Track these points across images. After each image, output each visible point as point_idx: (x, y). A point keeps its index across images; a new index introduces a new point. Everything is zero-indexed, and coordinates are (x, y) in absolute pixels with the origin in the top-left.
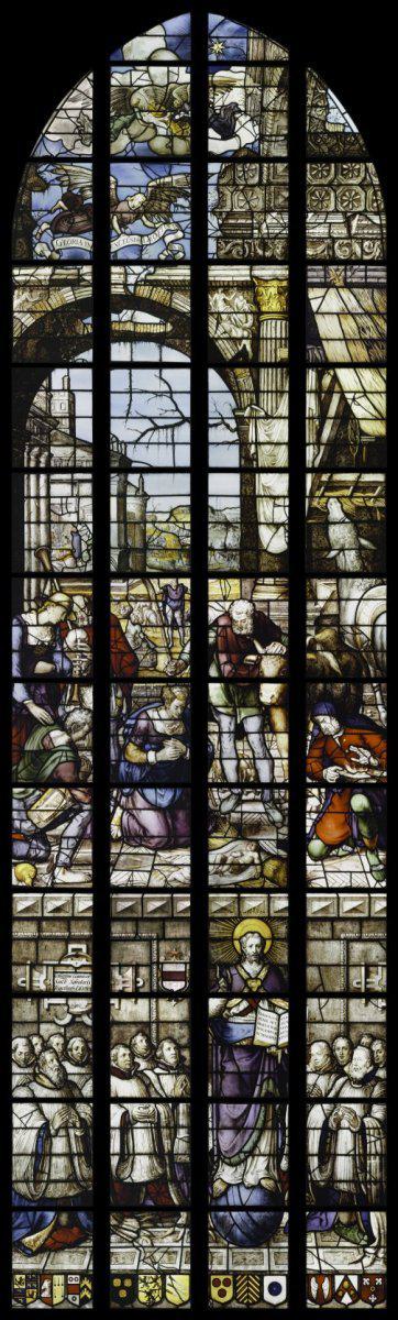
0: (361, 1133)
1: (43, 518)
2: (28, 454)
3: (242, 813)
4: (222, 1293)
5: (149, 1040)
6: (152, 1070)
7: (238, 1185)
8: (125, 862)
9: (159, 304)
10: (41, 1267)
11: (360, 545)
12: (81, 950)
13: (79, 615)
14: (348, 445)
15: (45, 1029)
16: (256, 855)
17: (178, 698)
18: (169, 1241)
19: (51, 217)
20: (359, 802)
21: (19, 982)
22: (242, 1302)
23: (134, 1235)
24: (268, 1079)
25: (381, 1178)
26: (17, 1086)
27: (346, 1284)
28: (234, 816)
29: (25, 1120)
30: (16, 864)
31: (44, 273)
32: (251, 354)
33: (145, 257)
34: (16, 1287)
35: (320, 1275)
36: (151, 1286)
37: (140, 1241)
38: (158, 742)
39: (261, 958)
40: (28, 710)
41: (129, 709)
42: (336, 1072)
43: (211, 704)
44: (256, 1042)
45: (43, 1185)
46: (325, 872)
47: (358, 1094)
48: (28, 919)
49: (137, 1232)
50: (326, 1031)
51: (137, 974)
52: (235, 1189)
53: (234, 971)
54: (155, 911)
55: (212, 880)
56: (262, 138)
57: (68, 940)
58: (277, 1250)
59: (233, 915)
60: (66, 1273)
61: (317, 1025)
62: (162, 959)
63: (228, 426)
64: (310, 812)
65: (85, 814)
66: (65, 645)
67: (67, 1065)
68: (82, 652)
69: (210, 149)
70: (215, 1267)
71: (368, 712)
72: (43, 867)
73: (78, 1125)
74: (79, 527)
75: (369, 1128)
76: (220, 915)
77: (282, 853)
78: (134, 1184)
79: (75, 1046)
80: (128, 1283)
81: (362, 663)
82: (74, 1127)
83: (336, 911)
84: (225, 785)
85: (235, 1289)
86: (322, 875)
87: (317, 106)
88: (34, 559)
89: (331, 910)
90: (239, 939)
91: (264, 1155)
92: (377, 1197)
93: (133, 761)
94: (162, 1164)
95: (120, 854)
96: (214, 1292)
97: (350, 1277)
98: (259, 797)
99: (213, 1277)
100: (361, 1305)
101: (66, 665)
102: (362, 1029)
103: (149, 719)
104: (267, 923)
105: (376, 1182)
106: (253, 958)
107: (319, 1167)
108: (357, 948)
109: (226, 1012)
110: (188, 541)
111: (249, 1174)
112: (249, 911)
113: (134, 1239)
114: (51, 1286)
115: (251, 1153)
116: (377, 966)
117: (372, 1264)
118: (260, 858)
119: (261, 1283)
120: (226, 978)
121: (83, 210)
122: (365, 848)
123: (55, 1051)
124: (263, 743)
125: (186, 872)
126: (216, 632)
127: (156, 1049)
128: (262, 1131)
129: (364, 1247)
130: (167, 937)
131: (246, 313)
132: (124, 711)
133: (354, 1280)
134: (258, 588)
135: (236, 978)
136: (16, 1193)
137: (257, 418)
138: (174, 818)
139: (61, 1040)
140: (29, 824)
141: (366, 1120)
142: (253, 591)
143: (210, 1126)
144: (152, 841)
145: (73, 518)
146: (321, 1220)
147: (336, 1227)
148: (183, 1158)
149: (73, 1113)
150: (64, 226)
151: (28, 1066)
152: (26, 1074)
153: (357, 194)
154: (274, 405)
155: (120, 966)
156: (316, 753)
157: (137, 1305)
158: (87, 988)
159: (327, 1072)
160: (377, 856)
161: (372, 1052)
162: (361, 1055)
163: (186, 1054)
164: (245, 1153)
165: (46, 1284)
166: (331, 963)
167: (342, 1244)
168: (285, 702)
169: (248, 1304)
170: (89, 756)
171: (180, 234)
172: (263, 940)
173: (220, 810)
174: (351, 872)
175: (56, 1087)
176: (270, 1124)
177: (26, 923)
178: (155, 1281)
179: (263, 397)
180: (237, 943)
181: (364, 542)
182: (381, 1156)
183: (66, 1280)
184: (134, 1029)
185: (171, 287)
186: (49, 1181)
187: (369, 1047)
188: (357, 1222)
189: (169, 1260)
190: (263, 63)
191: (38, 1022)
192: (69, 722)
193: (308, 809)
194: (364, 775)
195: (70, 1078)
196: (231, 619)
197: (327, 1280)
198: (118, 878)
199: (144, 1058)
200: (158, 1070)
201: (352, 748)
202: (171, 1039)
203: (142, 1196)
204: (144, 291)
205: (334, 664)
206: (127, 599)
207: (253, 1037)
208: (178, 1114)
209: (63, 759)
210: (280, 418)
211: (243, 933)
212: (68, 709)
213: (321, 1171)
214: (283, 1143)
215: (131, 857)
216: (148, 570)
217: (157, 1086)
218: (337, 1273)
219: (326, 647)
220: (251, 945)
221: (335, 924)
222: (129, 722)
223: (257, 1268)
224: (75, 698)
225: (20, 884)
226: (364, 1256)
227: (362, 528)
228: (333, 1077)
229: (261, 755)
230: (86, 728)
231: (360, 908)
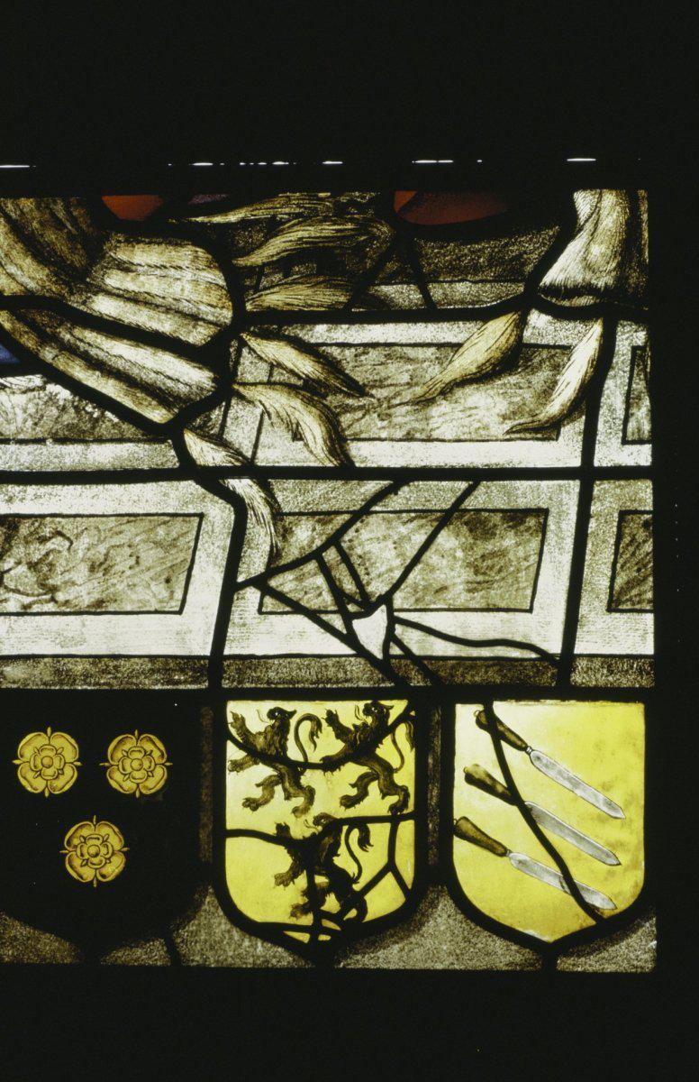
23: (193, 377)
36: (330, 791)
37: (241, 426)
178: (361, 746)
189: (484, 572)
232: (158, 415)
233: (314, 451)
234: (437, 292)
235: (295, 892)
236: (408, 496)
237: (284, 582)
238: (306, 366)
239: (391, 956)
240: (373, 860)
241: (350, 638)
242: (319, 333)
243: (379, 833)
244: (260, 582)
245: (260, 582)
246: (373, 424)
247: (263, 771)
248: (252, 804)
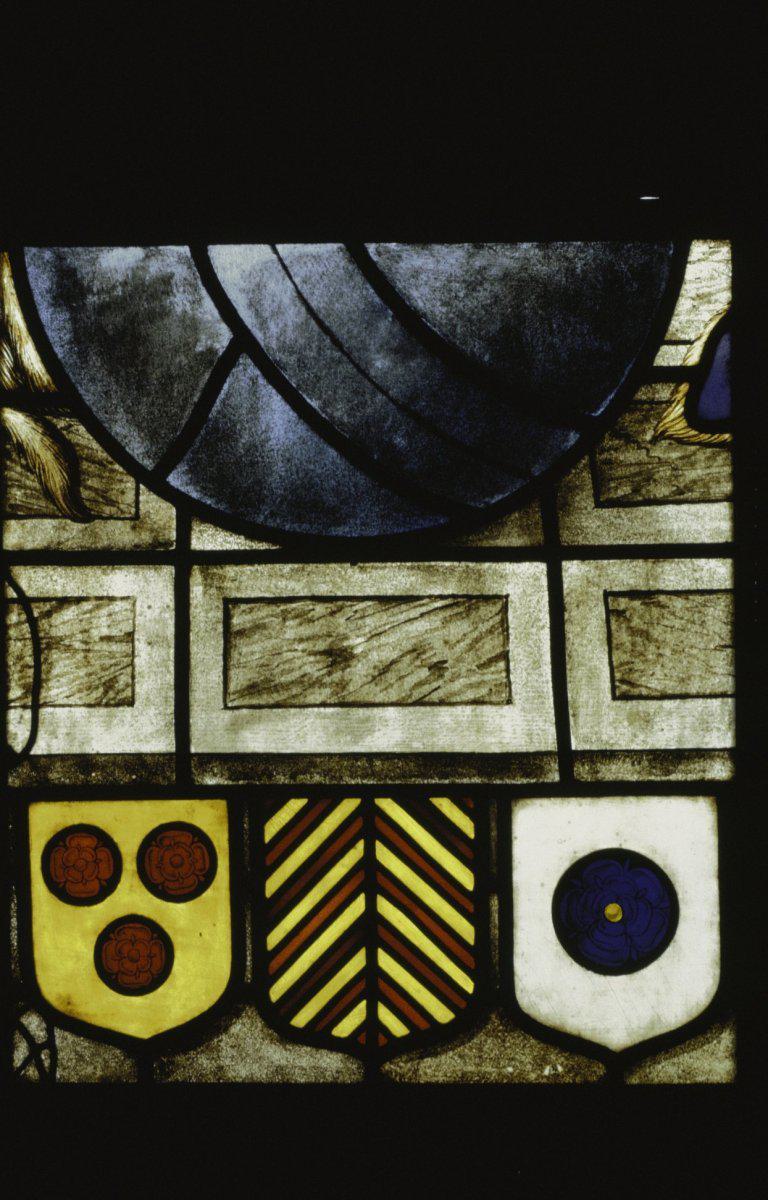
22: (318, 1036)
58: (625, 574)
99: (45, 820)
169: (370, 1044)
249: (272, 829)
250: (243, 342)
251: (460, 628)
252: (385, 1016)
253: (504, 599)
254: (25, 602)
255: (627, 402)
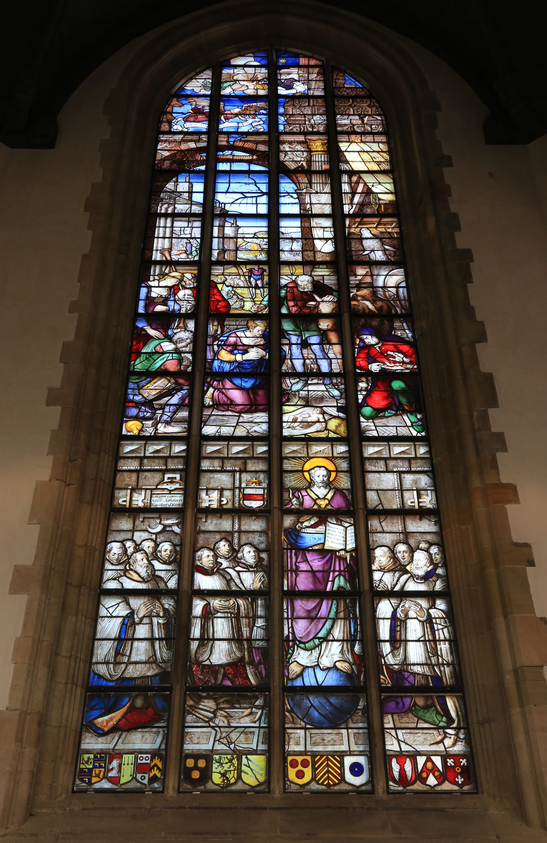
0: (429, 621)
1: (168, 235)
2: (161, 207)
3: (308, 391)
4: (300, 775)
5: (231, 545)
6: (233, 568)
7: (313, 667)
8: (214, 420)
9: (249, 148)
10: (111, 746)
11: (385, 248)
12: (175, 478)
13: (188, 283)
14: (372, 204)
15: (138, 536)
16: (321, 416)
17: (259, 328)
18: (246, 722)
19: (184, 116)
20: (397, 385)
21: (120, 501)
22: (322, 784)
23: (211, 715)
24: (339, 575)
25: (453, 661)
26: (108, 580)
27: (429, 765)
28: (303, 393)
29: (111, 610)
30: (126, 421)
31: (179, 137)
32: (306, 167)
33: (240, 130)
34: (82, 766)
35: (401, 756)
36: (226, 767)
37: (217, 721)
38: (245, 349)
39: (328, 484)
40: (146, 331)
41: (222, 331)
42: (399, 570)
43: (284, 329)
44: (326, 547)
45: (123, 666)
46: (376, 426)
47: (422, 587)
48: (132, 458)
49: (214, 713)
50: (388, 539)
51: (221, 496)
52: (311, 671)
53: (304, 493)
54: (238, 453)
55: (286, 432)
56: (309, 89)
57: (164, 472)
58: (356, 731)
59: (302, 455)
60: (136, 752)
61: (379, 535)
62: (244, 485)
63: (292, 197)
64: (361, 390)
65: (184, 392)
66: (176, 297)
67: (156, 564)
68: (188, 301)
69: (279, 93)
70: (292, 747)
71: (399, 333)
72: (149, 423)
73: (161, 614)
74: (191, 240)
75: (436, 618)
76: (292, 455)
77: (341, 415)
78: (212, 667)
79: (164, 549)
80: (202, 763)
81: (391, 306)
82: (158, 616)
83: (388, 453)
84: (295, 374)
85: (314, 769)
86: (374, 428)
87: (339, 79)
88: (159, 254)
89: (384, 453)
90: (308, 471)
91: (338, 641)
92: (451, 677)
93: (224, 360)
94: (241, 649)
95: (210, 415)
96: (292, 773)
97: (433, 758)
98: (321, 382)
99: (290, 758)
100: (447, 786)
101: (177, 307)
102: (419, 537)
103: (238, 337)
104: (331, 461)
105: (448, 664)
106: (321, 485)
107: (392, 651)
108: (408, 479)
109: (299, 525)
110: (266, 247)
111: (324, 657)
112: (316, 453)
113: (211, 719)
114: (120, 766)
115: (325, 639)
116: (427, 490)
117: (454, 744)
118: (324, 418)
119: (342, 763)
120: (298, 498)
121: (203, 113)
122: (405, 412)
123: (146, 552)
124: (323, 350)
125: (265, 427)
126: (286, 290)
127: (237, 552)
128: (334, 620)
129: (444, 728)
130: (248, 470)
131: (302, 151)
132: (219, 332)
133: (437, 761)
134: (315, 270)
135: (307, 498)
136: (95, 674)
137: (310, 193)
138: (255, 394)
139: (152, 544)
140: (140, 397)
141: (432, 611)
142: (312, 271)
143: (285, 615)
144: (237, 407)
145: (189, 236)
146: (397, 703)
147: (411, 710)
148: (261, 643)
149: (158, 604)
150: (192, 119)
151: (120, 564)
152: (117, 570)
153: (366, 109)
154: (321, 188)
155: (207, 489)
156: (363, 355)
157: (210, 786)
158: (179, 505)
159: (393, 571)
160: (416, 417)
161: (430, 555)
162: (420, 557)
163: (264, 555)
164: (319, 638)
165: (115, 763)
166: (387, 488)
167: (420, 725)
168: (338, 328)
169: (328, 785)
170: (189, 356)
171: (262, 122)
172: (329, 472)
173: (291, 390)
174: (396, 427)
175: (144, 580)
176: (342, 615)
177: (130, 460)
178: (230, 761)
179: (313, 185)
180: (306, 474)
181: (386, 247)
182: (450, 641)
183: (136, 758)
184: (218, 537)
185: (257, 143)
186: (129, 663)
187: (427, 551)
188: (433, 705)
189: (246, 739)
190: (308, 66)
191: (133, 531)
192: (175, 338)
193: (359, 388)
194: (400, 368)
195: (158, 573)
196: (297, 284)
197: (408, 760)
198: (209, 430)
199: (226, 558)
200: (238, 569)
201: (389, 353)
202: (251, 544)
203: (220, 677)
204: (240, 144)
205: (371, 306)
206: (223, 274)
207: (324, 544)
208: (257, 606)
209: (171, 358)
210: (326, 193)
211: (312, 467)
212: (175, 331)
213: (394, 656)
214: (356, 630)
215: (221, 417)
216: (238, 260)
217: (237, 581)
218: (420, 754)
219: (364, 298)
220: (319, 475)
221: (388, 462)
222: (222, 338)
223: (337, 748)
224: (181, 325)
225: (129, 434)
226: (445, 737)
227: (385, 241)
228: (397, 574)
229: (321, 357)
230: (189, 341)
231: (408, 452)
232: (207, 720)
233: (226, 724)
234: (242, 706)
235: (221, 780)
236: (237, 730)
237: (222, 740)
238: (225, 714)
239: (233, 788)
240: (231, 776)
241: (229, 747)
242: (227, 710)
243: (232, 772)
244: (218, 740)
245: (218, 740)
246: (233, 721)
247: (218, 764)
248: (216, 768)
249: (316, 759)
250: (312, 705)
251: (337, 737)
252: (330, 782)
253: (342, 733)
254: (288, 733)
255: (355, 712)
